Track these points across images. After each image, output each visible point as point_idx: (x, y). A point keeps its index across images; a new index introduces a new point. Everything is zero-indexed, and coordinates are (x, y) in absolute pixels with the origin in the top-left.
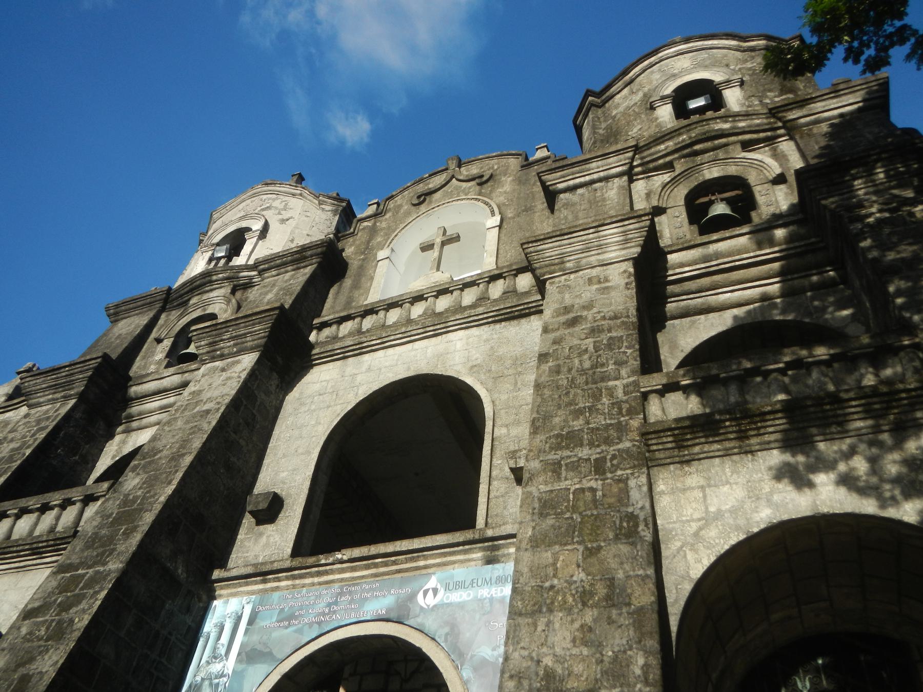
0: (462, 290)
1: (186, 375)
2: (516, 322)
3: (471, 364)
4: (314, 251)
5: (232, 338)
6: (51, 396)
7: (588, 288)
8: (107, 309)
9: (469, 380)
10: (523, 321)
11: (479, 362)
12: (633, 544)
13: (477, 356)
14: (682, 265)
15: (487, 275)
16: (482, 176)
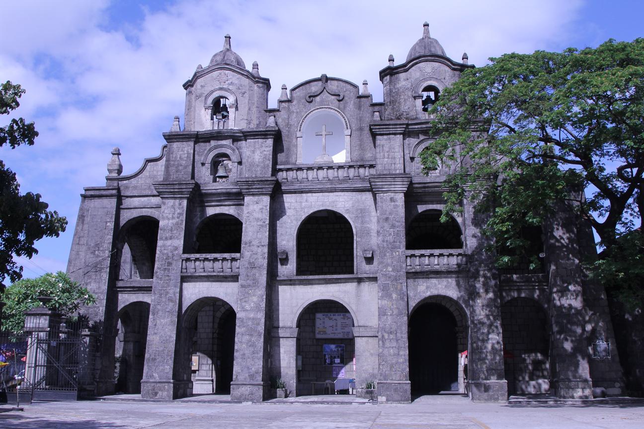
0: (338, 169)
1: (228, 190)
2: (361, 193)
3: (346, 209)
4: (273, 133)
5: (255, 188)
6: (172, 196)
7: (390, 203)
8: (164, 136)
9: (346, 216)
10: (363, 193)
11: (348, 208)
12: (403, 301)
13: (349, 205)
14: (417, 188)
15: (348, 165)
16: (339, 95)
